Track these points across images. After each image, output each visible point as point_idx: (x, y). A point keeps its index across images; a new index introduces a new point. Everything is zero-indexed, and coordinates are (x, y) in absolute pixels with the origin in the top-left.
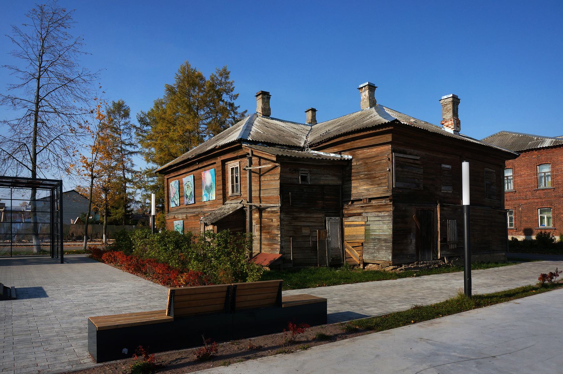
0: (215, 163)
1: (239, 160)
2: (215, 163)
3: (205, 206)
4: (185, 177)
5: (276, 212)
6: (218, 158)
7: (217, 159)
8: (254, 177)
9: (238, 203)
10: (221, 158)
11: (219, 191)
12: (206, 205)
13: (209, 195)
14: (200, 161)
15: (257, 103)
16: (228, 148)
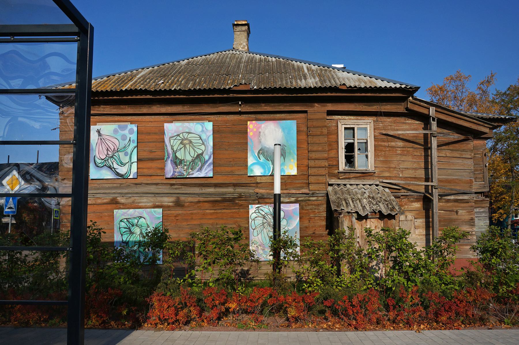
0: (306, 112)
1: (375, 118)
2: (306, 112)
3: (254, 185)
4: (172, 122)
5: (466, 201)
6: (316, 105)
7: (314, 106)
8: (412, 149)
9: (372, 185)
10: (324, 106)
11: (316, 161)
12: (258, 183)
13: (272, 166)
14: (246, 101)
15: (235, 36)
16: (369, 95)
